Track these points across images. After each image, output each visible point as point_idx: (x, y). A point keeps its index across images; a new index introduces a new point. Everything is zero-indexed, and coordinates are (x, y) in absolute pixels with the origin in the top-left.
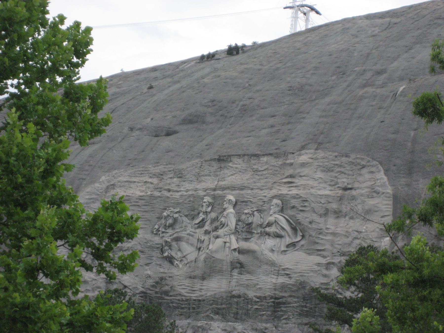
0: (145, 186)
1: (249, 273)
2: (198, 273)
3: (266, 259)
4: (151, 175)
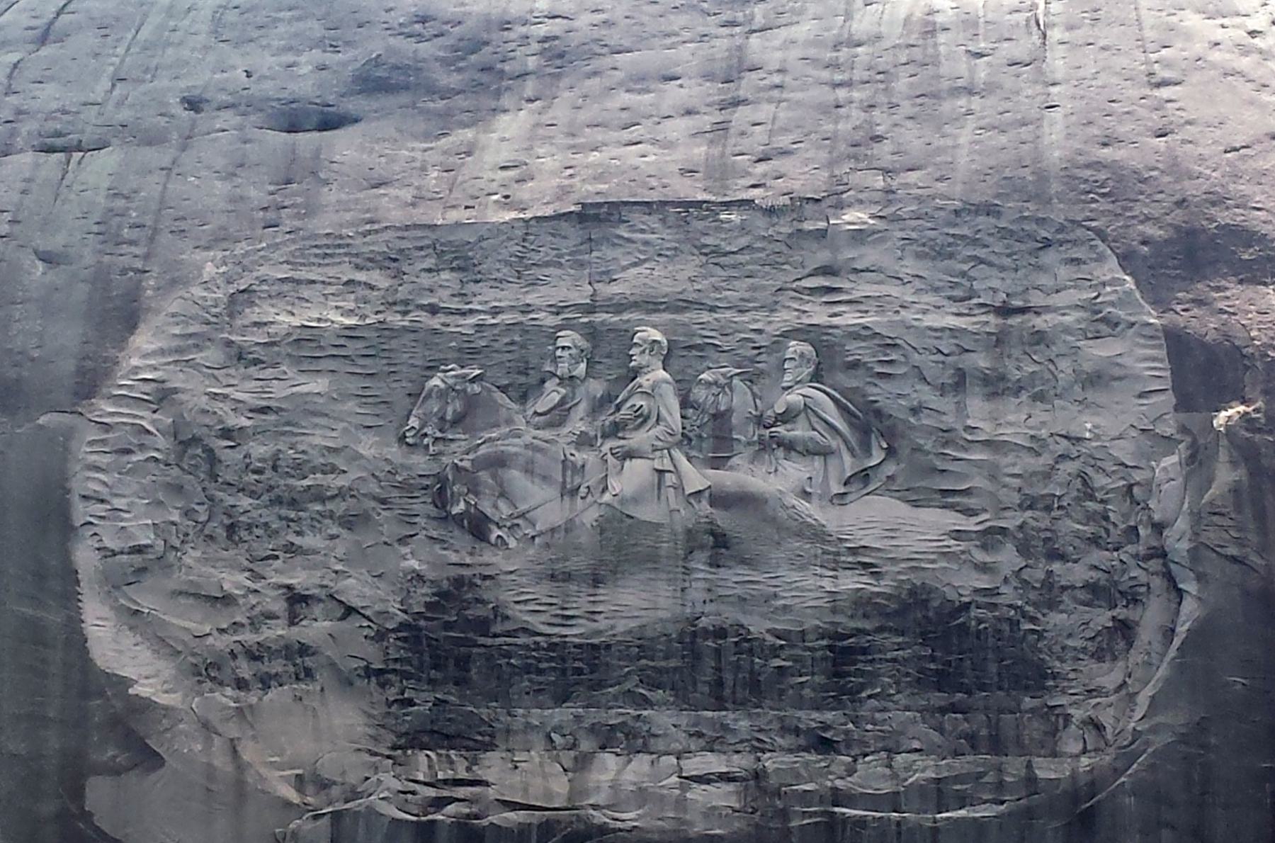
0: (352, 296)
1: (743, 562)
2: (577, 563)
3: (797, 520)
4: (358, 261)
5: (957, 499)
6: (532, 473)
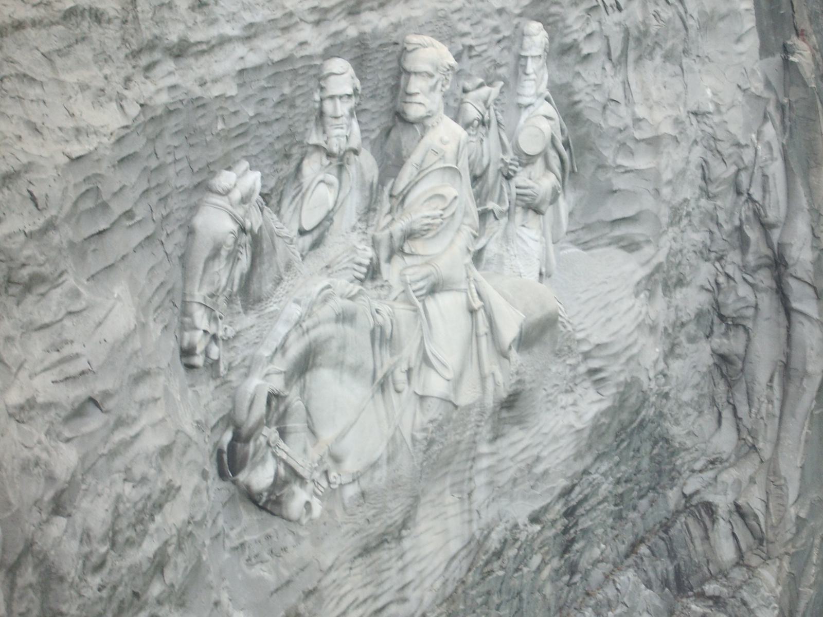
6: (342, 363)
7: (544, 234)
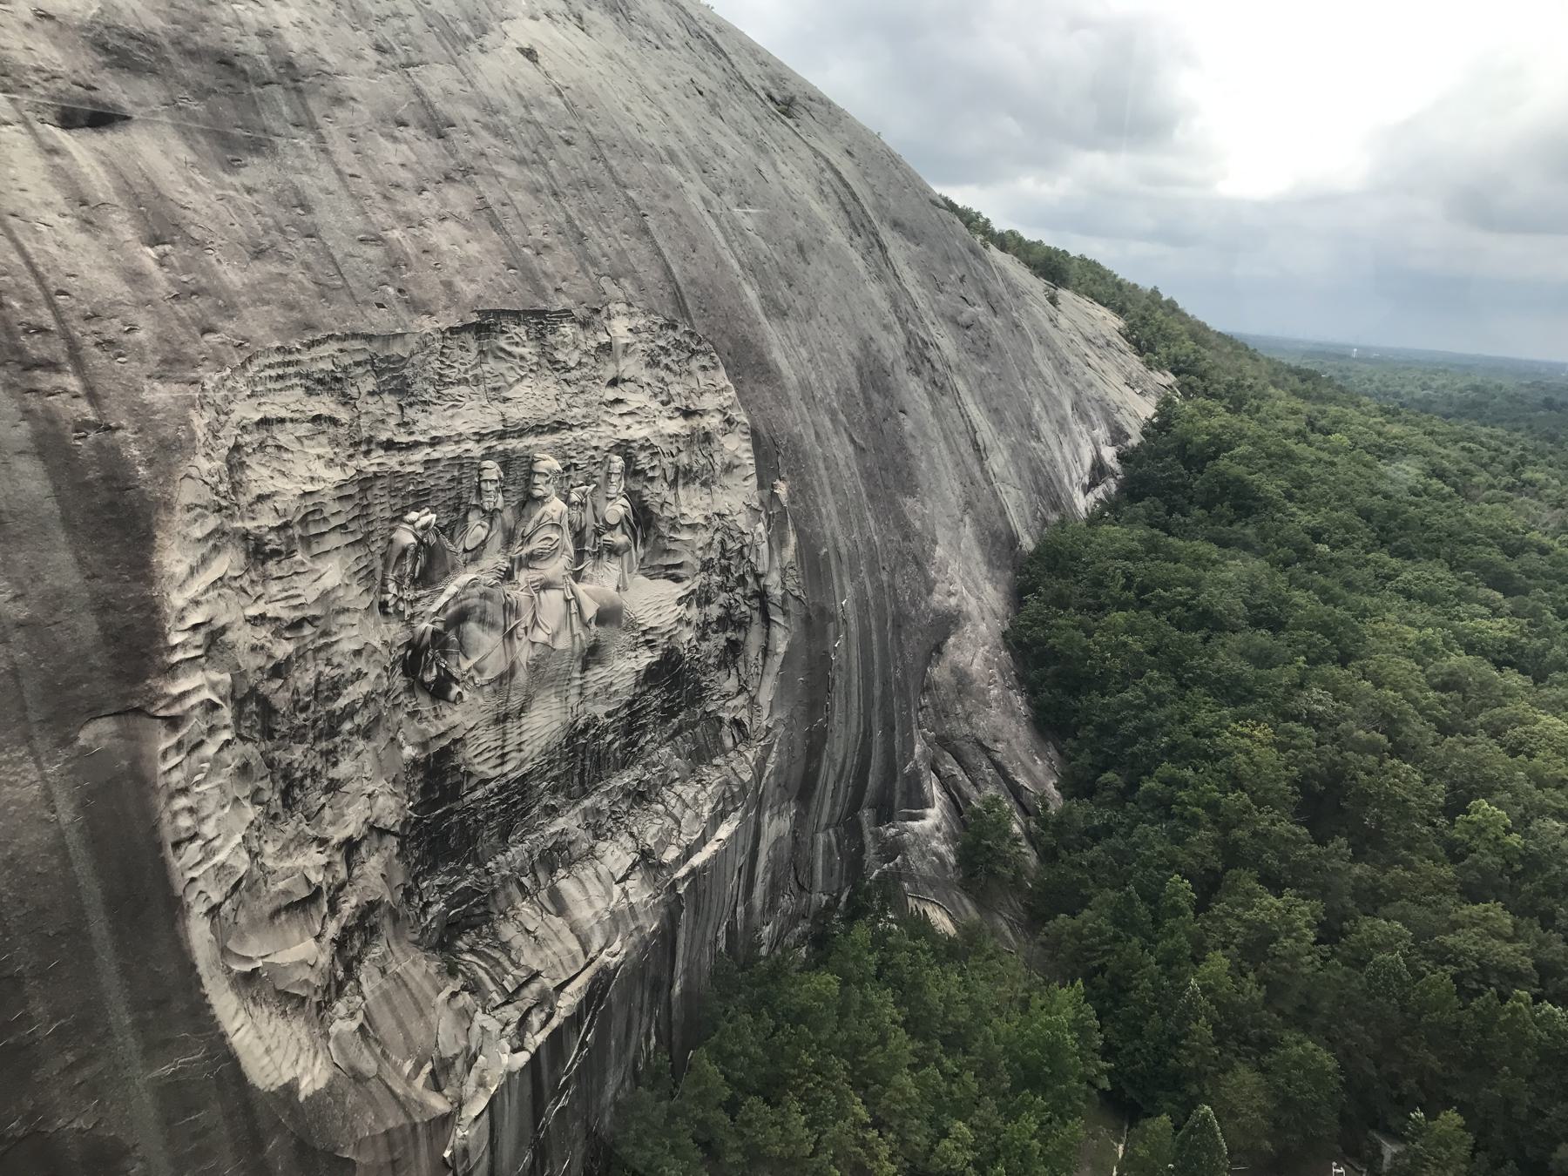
4: (309, 383)
5: (673, 571)
7: (622, 567)
